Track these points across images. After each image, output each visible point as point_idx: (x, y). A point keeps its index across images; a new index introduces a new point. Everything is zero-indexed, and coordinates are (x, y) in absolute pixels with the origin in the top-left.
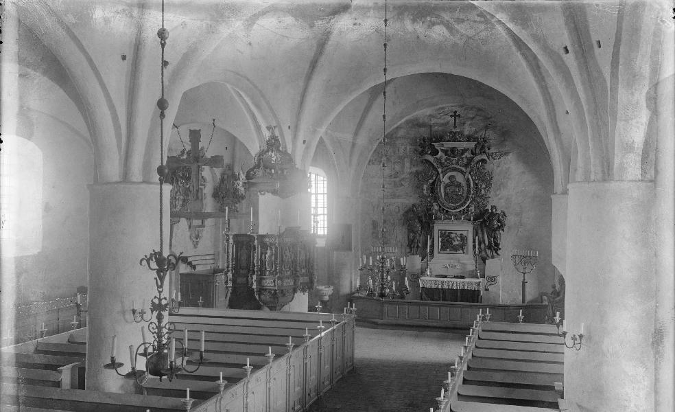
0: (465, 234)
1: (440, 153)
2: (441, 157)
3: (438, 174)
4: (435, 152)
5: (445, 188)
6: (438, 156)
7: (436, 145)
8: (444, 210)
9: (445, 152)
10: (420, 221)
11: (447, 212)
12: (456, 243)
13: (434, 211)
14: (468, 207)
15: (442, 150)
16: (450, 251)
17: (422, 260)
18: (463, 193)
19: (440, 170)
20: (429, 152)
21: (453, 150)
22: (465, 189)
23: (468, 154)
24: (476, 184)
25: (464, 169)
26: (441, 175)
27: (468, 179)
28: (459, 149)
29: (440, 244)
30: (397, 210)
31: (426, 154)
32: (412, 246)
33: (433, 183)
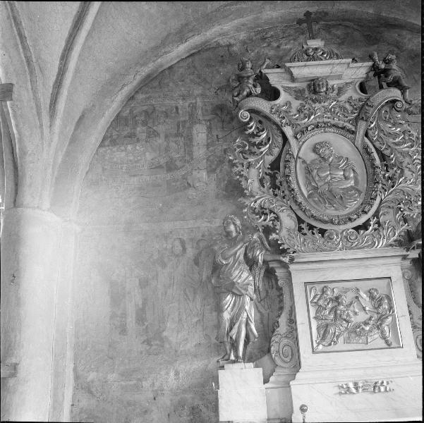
0: (381, 287)
1: (284, 97)
2: (288, 104)
3: (285, 139)
4: (271, 94)
5: (308, 171)
6: (280, 101)
7: (276, 78)
8: (311, 227)
9: (298, 94)
10: (251, 263)
11: (322, 232)
12: (362, 317)
13: (284, 233)
14: (376, 215)
15: (287, 89)
16: (347, 341)
17: (266, 381)
18: (356, 182)
19: (289, 131)
20: (259, 90)
21: (314, 86)
22: (361, 170)
23: (353, 93)
24: (383, 157)
25: (349, 126)
26: (292, 141)
27: (366, 148)
28: (331, 83)
29: (314, 324)
30: (178, 248)
31: (250, 95)
32: (234, 333)
33: (275, 165)
